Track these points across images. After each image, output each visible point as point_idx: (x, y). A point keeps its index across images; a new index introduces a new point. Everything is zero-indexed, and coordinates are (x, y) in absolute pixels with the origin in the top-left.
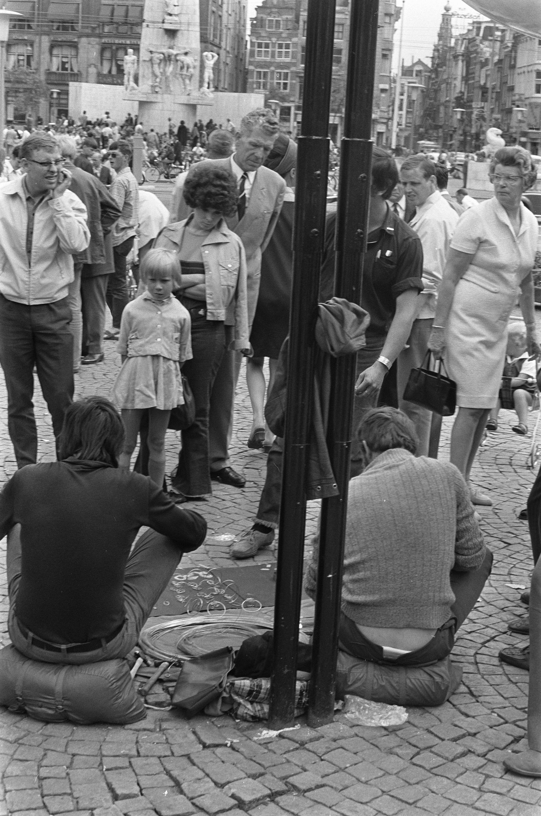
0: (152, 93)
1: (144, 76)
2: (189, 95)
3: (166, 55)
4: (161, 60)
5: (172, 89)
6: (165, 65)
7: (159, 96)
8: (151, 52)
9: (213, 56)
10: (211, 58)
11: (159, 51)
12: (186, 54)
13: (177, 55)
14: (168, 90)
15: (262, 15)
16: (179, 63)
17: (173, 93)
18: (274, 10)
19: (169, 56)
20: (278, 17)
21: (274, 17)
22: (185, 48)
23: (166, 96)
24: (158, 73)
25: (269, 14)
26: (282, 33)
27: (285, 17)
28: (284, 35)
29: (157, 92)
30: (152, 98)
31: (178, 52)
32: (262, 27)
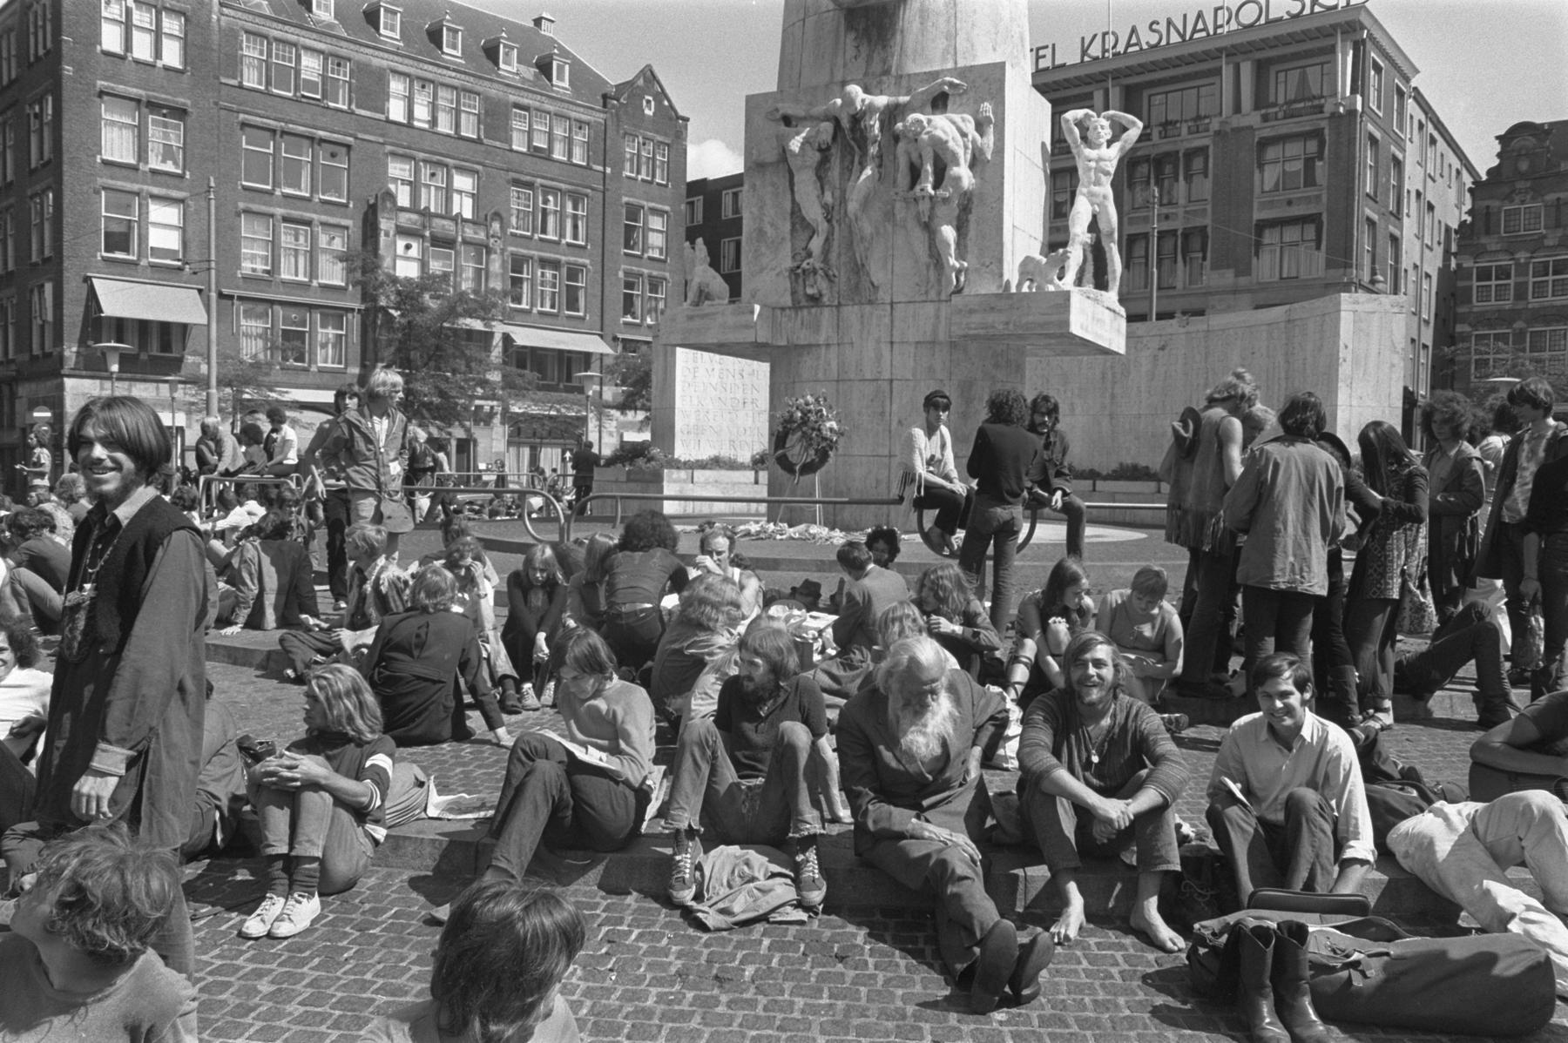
0: (796, 307)
1: (761, 232)
2: (959, 291)
3: (845, 124)
4: (824, 151)
5: (877, 274)
6: (849, 171)
7: (827, 315)
8: (787, 120)
9: (1119, 130)
10: (1106, 133)
11: (819, 109)
12: (939, 102)
13: (892, 114)
14: (860, 288)
15: (1486, 203)
16: (901, 146)
17: (883, 295)
18: (1520, 185)
19: (857, 119)
20: (1534, 199)
21: (1523, 202)
22: (934, 75)
23: (851, 312)
24: (813, 213)
25: (1509, 198)
26: (1544, 237)
27: (1551, 197)
28: (1549, 242)
29: (815, 300)
30: (795, 330)
31: (904, 99)
32: (1488, 232)
